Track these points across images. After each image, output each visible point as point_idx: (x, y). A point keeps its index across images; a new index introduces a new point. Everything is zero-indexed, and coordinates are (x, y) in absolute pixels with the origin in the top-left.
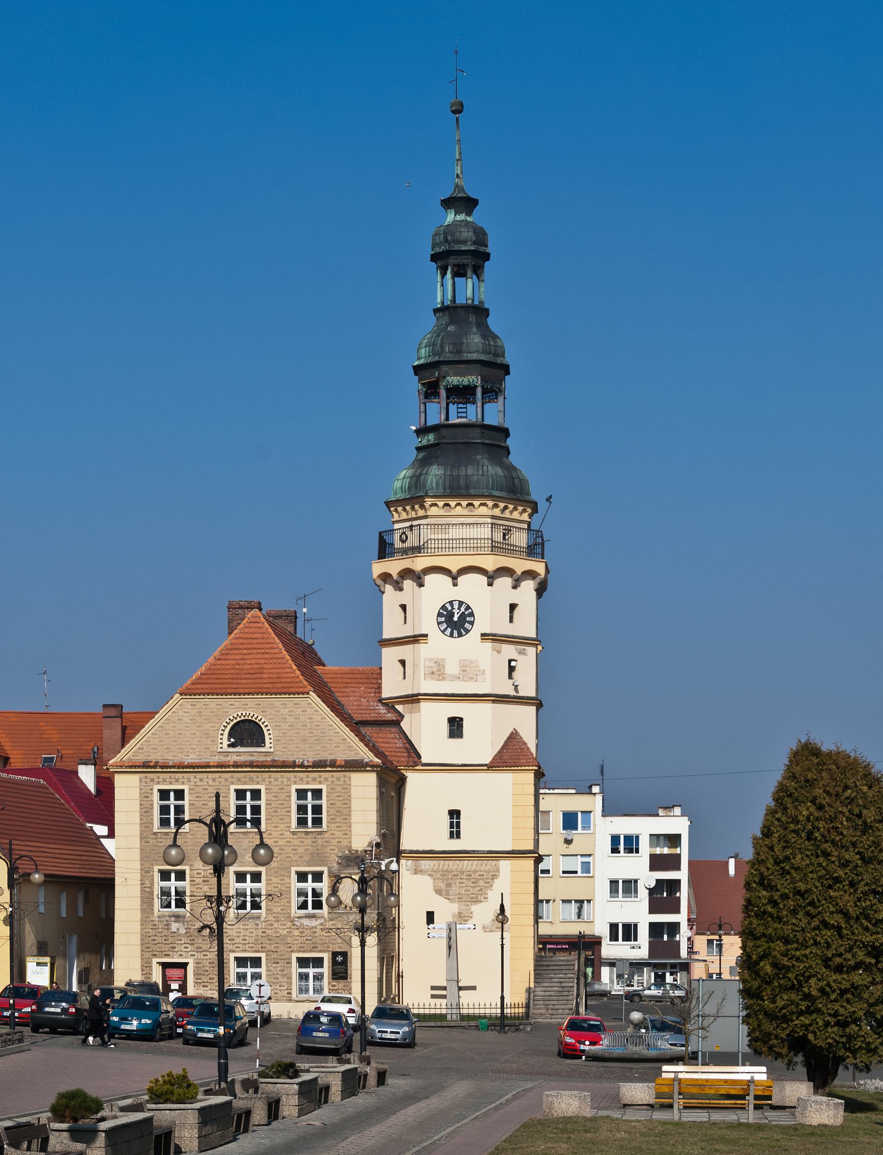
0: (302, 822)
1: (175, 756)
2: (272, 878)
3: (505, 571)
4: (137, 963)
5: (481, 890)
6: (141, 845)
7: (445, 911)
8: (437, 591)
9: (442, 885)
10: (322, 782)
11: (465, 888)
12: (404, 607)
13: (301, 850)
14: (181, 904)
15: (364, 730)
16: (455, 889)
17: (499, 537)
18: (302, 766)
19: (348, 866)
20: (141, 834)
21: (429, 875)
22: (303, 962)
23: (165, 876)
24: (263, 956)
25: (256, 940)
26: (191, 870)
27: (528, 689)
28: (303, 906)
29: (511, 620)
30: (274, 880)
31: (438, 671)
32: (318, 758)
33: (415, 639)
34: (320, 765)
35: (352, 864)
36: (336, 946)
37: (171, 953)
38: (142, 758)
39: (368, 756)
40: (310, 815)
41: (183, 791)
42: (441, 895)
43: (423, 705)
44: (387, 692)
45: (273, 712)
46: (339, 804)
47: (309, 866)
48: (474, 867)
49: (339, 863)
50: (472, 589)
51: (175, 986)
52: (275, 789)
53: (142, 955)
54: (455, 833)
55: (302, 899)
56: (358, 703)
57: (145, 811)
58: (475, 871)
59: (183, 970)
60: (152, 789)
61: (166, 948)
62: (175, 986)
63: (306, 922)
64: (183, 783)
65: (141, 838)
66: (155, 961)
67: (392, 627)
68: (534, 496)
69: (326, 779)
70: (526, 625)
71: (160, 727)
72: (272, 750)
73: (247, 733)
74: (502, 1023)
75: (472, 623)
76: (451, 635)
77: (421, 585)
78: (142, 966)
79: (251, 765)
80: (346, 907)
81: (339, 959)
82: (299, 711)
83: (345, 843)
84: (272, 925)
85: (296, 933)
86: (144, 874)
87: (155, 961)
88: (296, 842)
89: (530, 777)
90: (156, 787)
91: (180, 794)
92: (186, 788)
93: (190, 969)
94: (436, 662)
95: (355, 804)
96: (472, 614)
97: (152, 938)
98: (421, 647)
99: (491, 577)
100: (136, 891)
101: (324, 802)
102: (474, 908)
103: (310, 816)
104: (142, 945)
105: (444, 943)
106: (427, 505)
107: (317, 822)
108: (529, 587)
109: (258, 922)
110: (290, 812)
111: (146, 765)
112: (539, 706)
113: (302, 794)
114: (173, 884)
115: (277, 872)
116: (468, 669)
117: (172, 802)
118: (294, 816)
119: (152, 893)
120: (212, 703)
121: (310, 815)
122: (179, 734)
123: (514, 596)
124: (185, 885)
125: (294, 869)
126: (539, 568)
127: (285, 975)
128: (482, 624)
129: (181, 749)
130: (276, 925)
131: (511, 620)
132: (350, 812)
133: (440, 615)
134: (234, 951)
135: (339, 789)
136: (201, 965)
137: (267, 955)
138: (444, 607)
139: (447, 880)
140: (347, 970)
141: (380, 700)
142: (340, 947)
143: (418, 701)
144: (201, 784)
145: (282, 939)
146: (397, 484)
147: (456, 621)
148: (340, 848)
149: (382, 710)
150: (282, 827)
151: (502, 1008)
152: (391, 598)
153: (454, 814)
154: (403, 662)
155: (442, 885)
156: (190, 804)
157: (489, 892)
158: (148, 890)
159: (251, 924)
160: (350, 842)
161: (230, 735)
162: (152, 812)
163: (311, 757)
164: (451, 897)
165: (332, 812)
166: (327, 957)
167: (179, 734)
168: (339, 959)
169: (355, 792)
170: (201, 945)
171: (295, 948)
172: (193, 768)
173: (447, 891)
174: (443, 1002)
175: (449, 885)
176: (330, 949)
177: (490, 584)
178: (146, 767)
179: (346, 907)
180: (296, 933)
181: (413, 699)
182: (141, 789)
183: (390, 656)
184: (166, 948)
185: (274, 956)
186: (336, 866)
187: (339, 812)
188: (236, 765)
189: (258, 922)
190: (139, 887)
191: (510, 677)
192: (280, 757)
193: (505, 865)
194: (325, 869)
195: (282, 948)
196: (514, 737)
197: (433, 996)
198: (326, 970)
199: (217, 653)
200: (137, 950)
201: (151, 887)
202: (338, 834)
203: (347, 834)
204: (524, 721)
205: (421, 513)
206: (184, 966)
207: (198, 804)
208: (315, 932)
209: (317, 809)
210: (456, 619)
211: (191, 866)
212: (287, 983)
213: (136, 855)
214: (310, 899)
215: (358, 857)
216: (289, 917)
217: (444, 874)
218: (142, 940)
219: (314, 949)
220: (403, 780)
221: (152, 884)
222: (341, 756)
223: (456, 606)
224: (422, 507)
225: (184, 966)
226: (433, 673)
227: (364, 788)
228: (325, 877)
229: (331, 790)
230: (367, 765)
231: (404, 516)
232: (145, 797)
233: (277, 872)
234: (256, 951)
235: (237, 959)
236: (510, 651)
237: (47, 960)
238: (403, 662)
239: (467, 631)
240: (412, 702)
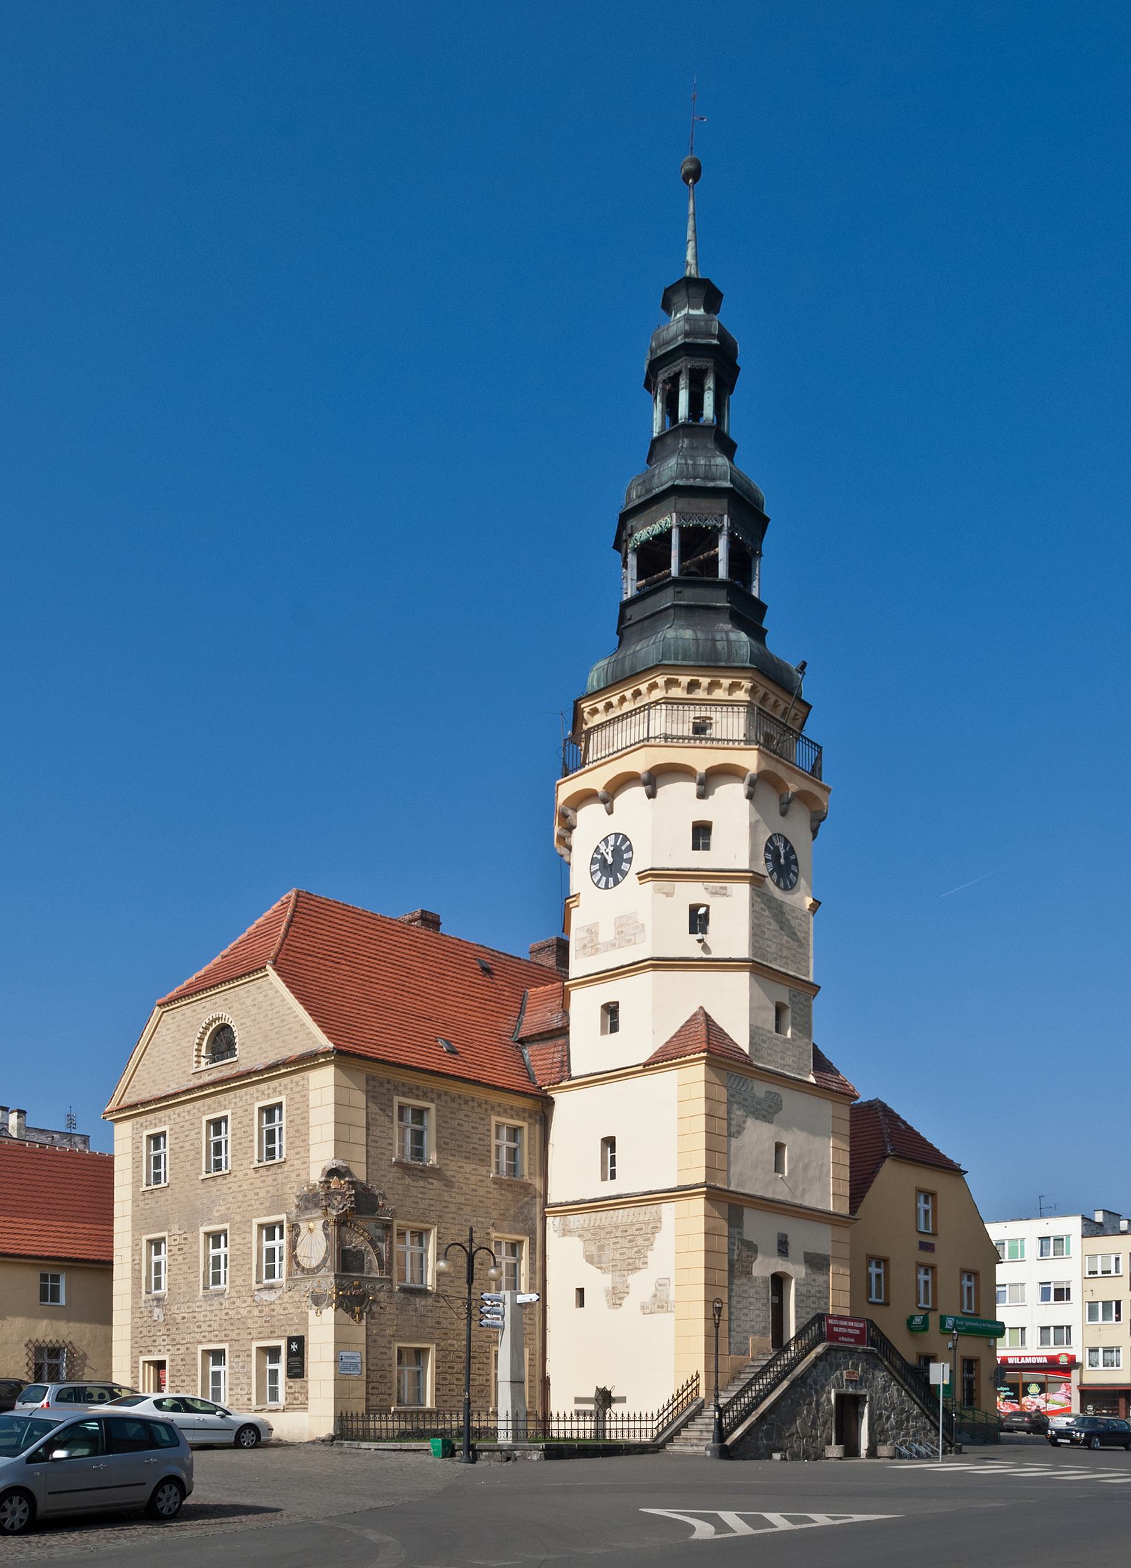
13: (262, 1193)
19: (306, 1208)
35: (310, 1205)
45: (239, 1007)
49: (297, 1206)
69: (286, 1088)
94: (588, 930)
109: (222, 1300)
115: (239, 1228)
116: (624, 929)
130: (238, 1302)
133: (593, 861)
134: (201, 1343)
135: (298, 1097)
142: (296, 1330)
166: (283, 1343)
168: (294, 1347)
180: (256, 1312)
185: (236, 1346)
186: (294, 1210)
187: (297, 1131)
189: (222, 1300)
208: (273, 1310)
210: (610, 860)
216: (250, 1290)
226: (585, 946)
233: (239, 1228)
236: (695, 892)
239: (624, 874)
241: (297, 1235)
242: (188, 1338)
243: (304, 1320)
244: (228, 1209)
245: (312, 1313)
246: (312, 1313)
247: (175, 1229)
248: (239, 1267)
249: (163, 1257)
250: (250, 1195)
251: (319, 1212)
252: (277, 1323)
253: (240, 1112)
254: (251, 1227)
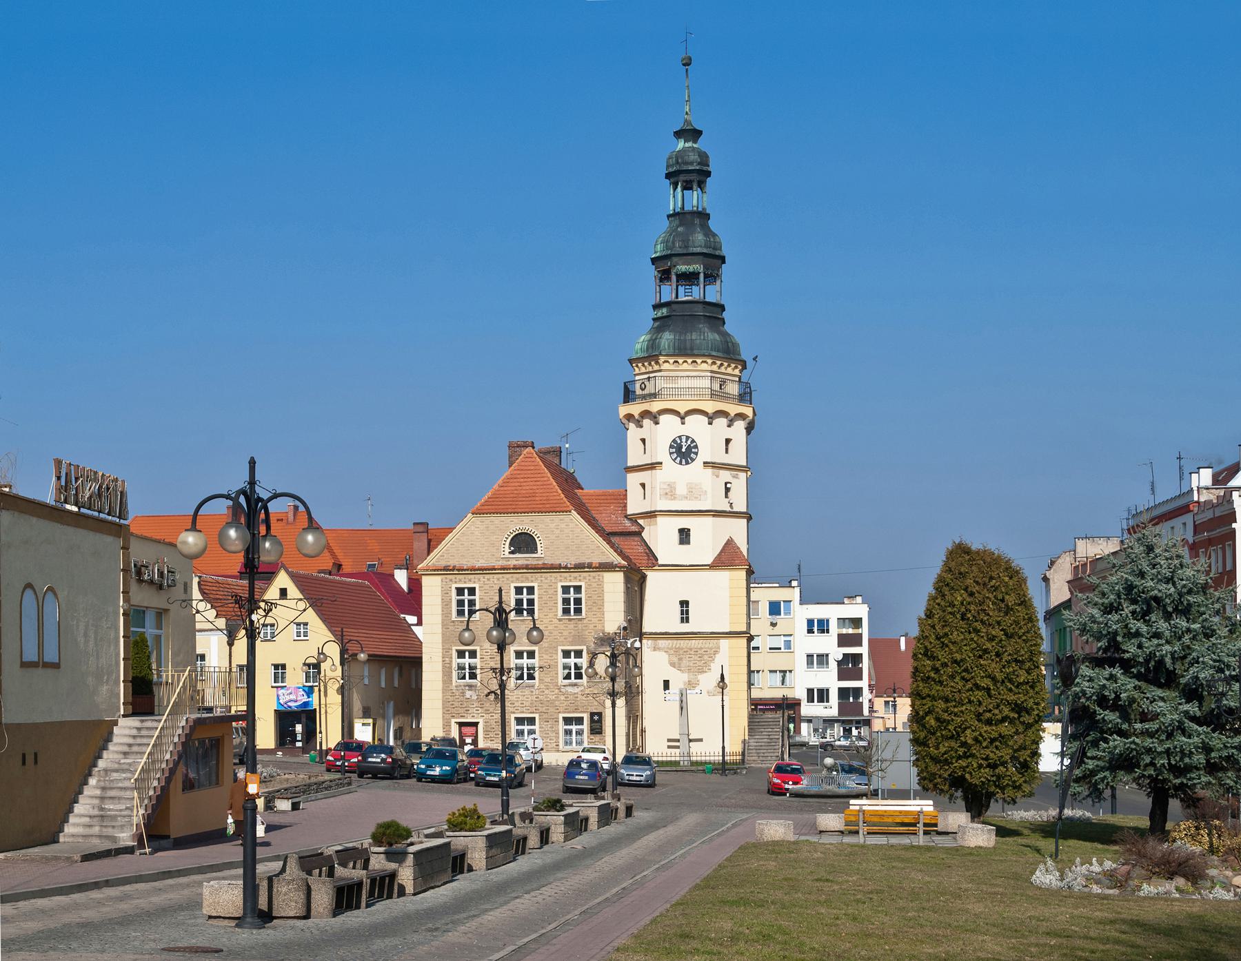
0: (566, 611)
3: (723, 413)
4: (440, 723)
7: (678, 680)
8: (669, 428)
9: (675, 660)
10: (581, 579)
12: (643, 441)
13: (565, 633)
14: (473, 676)
15: (614, 539)
16: (685, 662)
17: (716, 387)
18: (566, 567)
22: (568, 721)
23: (461, 654)
24: (537, 716)
27: (741, 506)
28: (568, 677)
29: (727, 452)
31: (670, 493)
32: (578, 561)
33: (653, 466)
34: (579, 567)
38: (443, 563)
39: (618, 560)
40: (573, 606)
41: (474, 589)
43: (659, 519)
44: (631, 510)
50: (696, 428)
51: (469, 740)
52: (545, 586)
54: (685, 618)
55: (567, 671)
56: (609, 519)
57: (446, 604)
61: (461, 711)
62: (469, 740)
63: (570, 689)
67: (635, 457)
68: (743, 357)
70: (738, 455)
73: (523, 542)
74: (723, 767)
75: (696, 454)
76: (680, 463)
77: (657, 423)
79: (527, 567)
82: (563, 526)
83: (599, 627)
85: (562, 698)
87: (453, 720)
88: (562, 627)
89: (742, 574)
90: (454, 586)
91: (472, 591)
92: (477, 586)
93: (480, 727)
95: (607, 597)
96: (696, 447)
98: (657, 472)
99: (711, 418)
100: (439, 667)
101: (583, 596)
102: (700, 677)
103: (572, 607)
105: (678, 703)
106: (661, 362)
107: (578, 611)
108: (740, 425)
111: (446, 569)
112: (749, 518)
113: (566, 589)
114: (467, 661)
117: (466, 597)
118: (560, 606)
119: (451, 668)
120: (497, 520)
121: (573, 606)
123: (729, 433)
124: (477, 661)
125: (560, 648)
126: (748, 411)
128: (704, 454)
131: (727, 452)
133: (671, 447)
138: (674, 441)
141: (626, 516)
143: (655, 516)
145: (551, 702)
146: (638, 346)
147: (684, 452)
149: (628, 523)
150: (551, 615)
151: (723, 756)
152: (633, 433)
153: (684, 604)
154: (643, 485)
155: (675, 660)
159: (527, 691)
161: (511, 545)
163: (573, 561)
165: (590, 603)
166: (586, 717)
168: (596, 718)
169: (607, 587)
172: (483, 570)
174: (677, 751)
175: (680, 659)
177: (710, 423)
178: (446, 570)
180: (562, 698)
181: (651, 515)
183: (633, 480)
184: (461, 711)
185: (545, 716)
188: (515, 568)
191: (726, 496)
192: (549, 561)
193: (724, 643)
194: (584, 648)
195: (552, 710)
196: (730, 543)
197: (669, 747)
198: (586, 726)
199: (500, 482)
200: (440, 712)
201: (451, 663)
203: (601, 620)
204: (738, 530)
205: (656, 367)
206: (475, 724)
207: (486, 599)
209: (578, 601)
213: (439, 638)
214: (573, 671)
217: (677, 650)
219: (576, 710)
220: (644, 577)
222: (596, 560)
223: (684, 439)
224: (657, 363)
225: (475, 724)
227: (614, 583)
228: (584, 654)
229: (589, 586)
230: (616, 566)
231: (643, 370)
232: (445, 593)
236: (726, 475)
237: (370, 721)
238: (643, 485)
239: (693, 460)
240: (650, 517)
250: (555, 633)
253: (545, 586)
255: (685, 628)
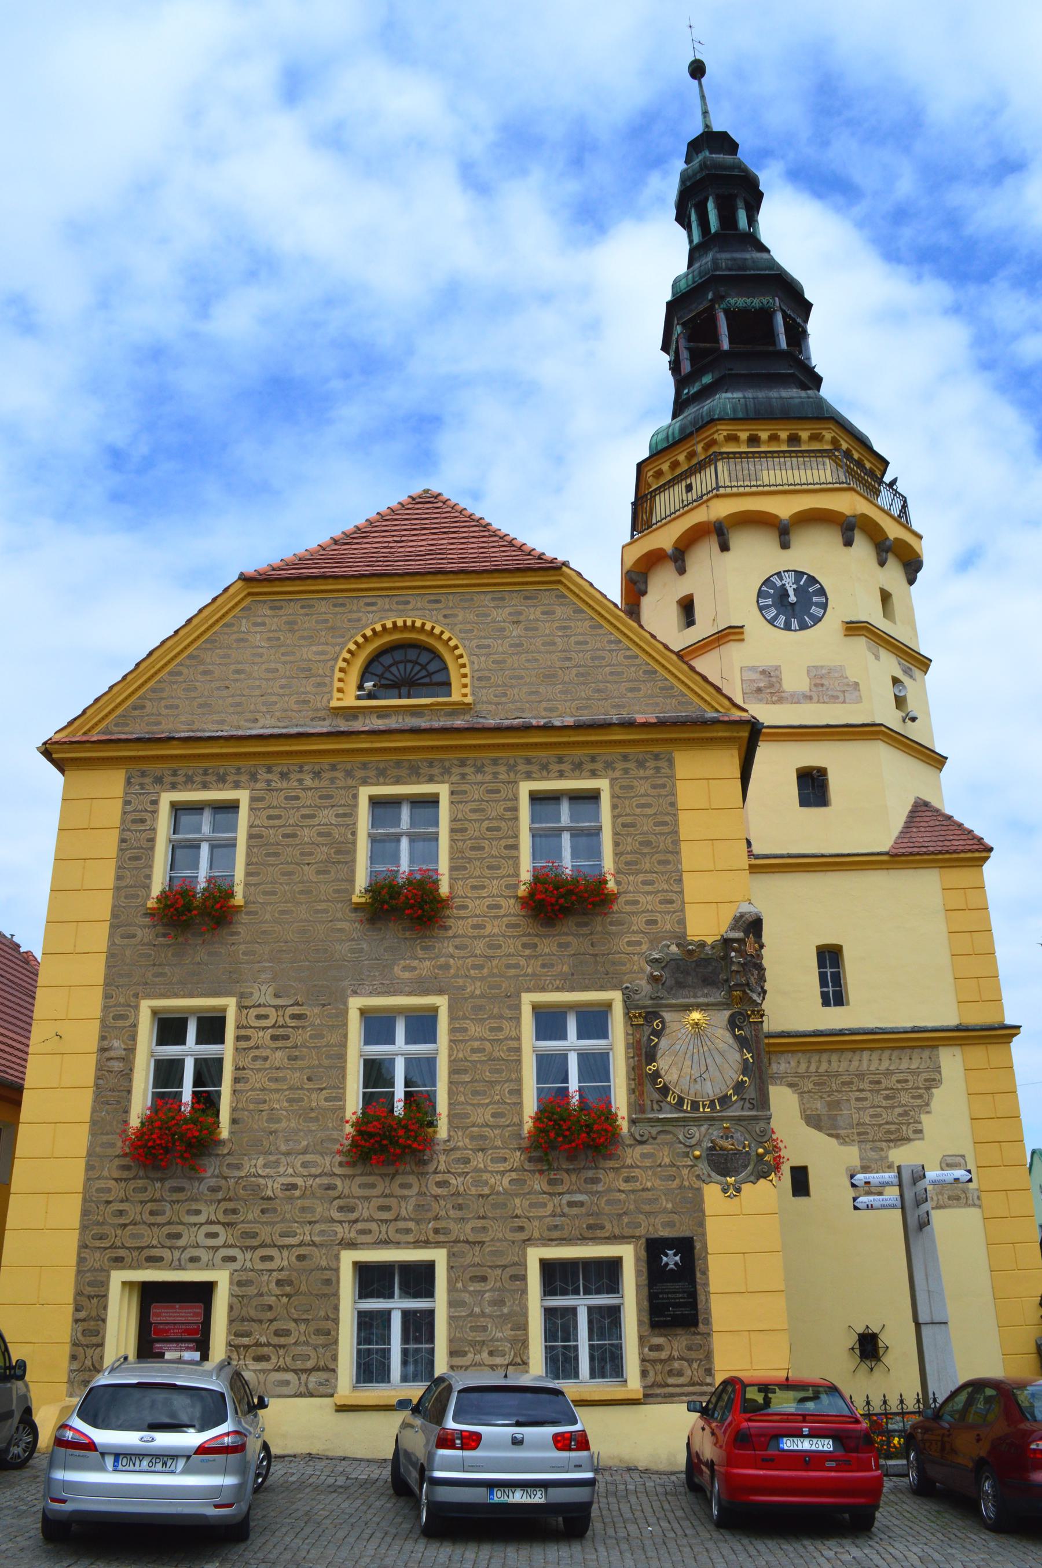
1: (222, 722)
2: (467, 1024)
5: (905, 1114)
6: (112, 943)
9: (819, 1106)
11: (871, 1111)
16: (849, 1112)
19: (680, 985)
20: (114, 915)
21: (790, 1085)
24: (439, 1257)
25: (418, 1207)
26: (241, 1007)
30: (474, 1030)
32: (586, 717)
35: (690, 980)
36: (659, 1221)
37: (166, 1253)
42: (818, 1127)
46: (647, 825)
47: (572, 989)
48: (885, 1064)
49: (654, 979)
53: (81, 1260)
54: (834, 994)
58: (888, 1073)
59: (199, 1308)
60: (155, 802)
61: (150, 1237)
64: (237, 786)
65: (113, 927)
66: (118, 1277)
69: (609, 766)
71: (189, 657)
72: (469, 699)
78: (79, 1293)
80: (681, 1101)
81: (671, 1259)
83: (667, 924)
84: (467, 1161)
86: (110, 1021)
87: (118, 1277)
97: (117, 1206)
100: (86, 1070)
104: (84, 1228)
110: (515, 847)
115: (481, 1008)
119: (127, 1075)
122: (237, 672)
127: (505, 1318)
129: (239, 704)
130: (479, 1160)
132: (676, 842)
134: (352, 1245)
136: (252, 1290)
137: (451, 1255)
139: (830, 1093)
140: (693, 1295)
142: (671, 1224)
144: (285, 785)
148: (654, 941)
156: (251, 837)
157: (924, 1117)
158: (117, 1066)
160: (682, 922)
162: (151, 858)
164: (842, 1132)
165: (630, 844)
167: (237, 672)
168: (671, 1259)
170: (256, 1228)
171: (535, 1229)
173: (833, 1118)
176: (641, 1231)
179: (681, 1101)
182: (127, 803)
184: (150, 1237)
185: (473, 1256)
187: (648, 843)
190: (93, 1059)
195: (497, 1231)
200: (68, 1246)
201: (128, 1057)
202: (647, 901)
203: (674, 901)
206: (204, 1292)
211: (242, 996)
212: (513, 1341)
213: (96, 970)
215: (707, 961)
218: (85, 1213)
221: (131, 1050)
225: (204, 1292)
233: (481, 1008)
234: (418, 1244)
235: (362, 1270)
241: (658, 1034)
242: (305, 1233)
243: (696, 1207)
244: (446, 967)
245: (712, 1193)
246: (712, 1193)
247: (263, 994)
248: (479, 1087)
249: (227, 1050)
251: (718, 996)
252: (607, 1209)
254: (518, 1007)
255: (835, 1019)
